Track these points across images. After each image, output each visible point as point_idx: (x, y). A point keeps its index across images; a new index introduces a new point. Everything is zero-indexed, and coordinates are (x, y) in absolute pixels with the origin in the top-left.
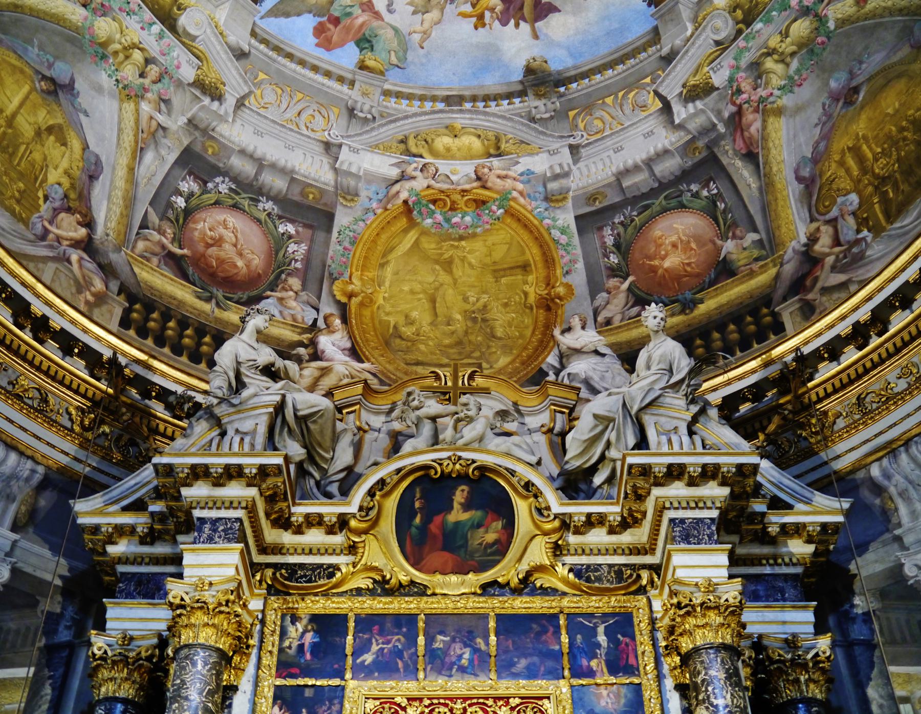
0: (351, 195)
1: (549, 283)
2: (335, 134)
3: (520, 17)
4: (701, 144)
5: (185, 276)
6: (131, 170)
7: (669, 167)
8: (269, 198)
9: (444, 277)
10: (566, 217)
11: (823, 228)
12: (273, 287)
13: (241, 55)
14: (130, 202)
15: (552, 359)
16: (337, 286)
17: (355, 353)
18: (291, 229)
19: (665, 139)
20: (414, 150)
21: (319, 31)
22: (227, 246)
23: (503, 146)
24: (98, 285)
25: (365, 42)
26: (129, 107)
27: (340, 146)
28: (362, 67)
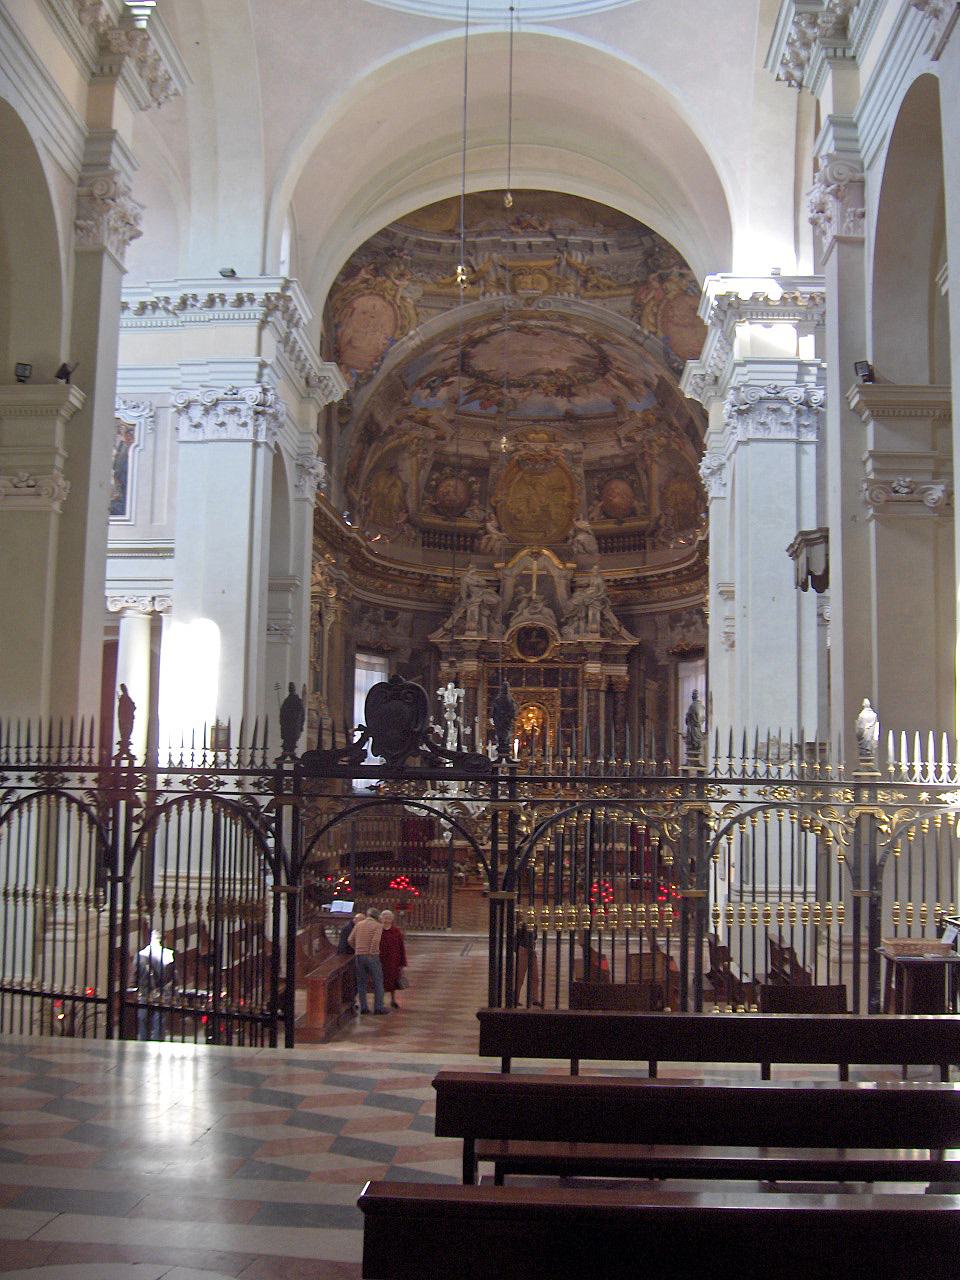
0: (495, 459)
1: (573, 497)
2: (488, 438)
3: (563, 395)
4: (631, 458)
5: (439, 513)
6: (417, 480)
7: (619, 461)
8: (465, 468)
9: (533, 492)
10: (580, 470)
11: (663, 517)
12: (468, 506)
13: (451, 421)
14: (418, 494)
15: (571, 532)
16: (492, 499)
17: (499, 529)
18: (473, 479)
19: (617, 451)
20: (520, 439)
21: (481, 405)
22: (451, 494)
23: (557, 439)
24: (414, 534)
25: (500, 404)
26: (414, 459)
27: (491, 442)
28: (499, 412)
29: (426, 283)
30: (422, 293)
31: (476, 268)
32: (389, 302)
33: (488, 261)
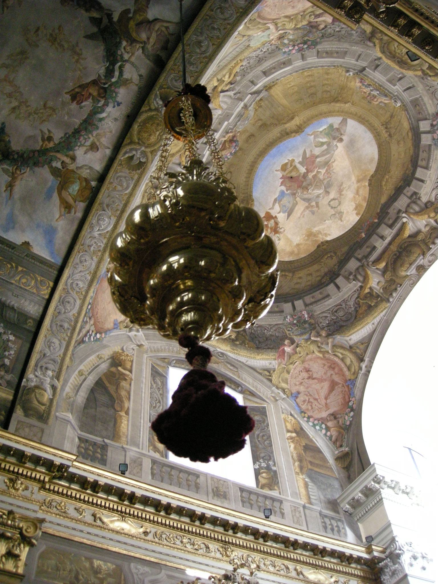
29: (255, 51)
30: (251, 46)
31: (222, 94)
32: (280, 19)
33: (220, 105)
